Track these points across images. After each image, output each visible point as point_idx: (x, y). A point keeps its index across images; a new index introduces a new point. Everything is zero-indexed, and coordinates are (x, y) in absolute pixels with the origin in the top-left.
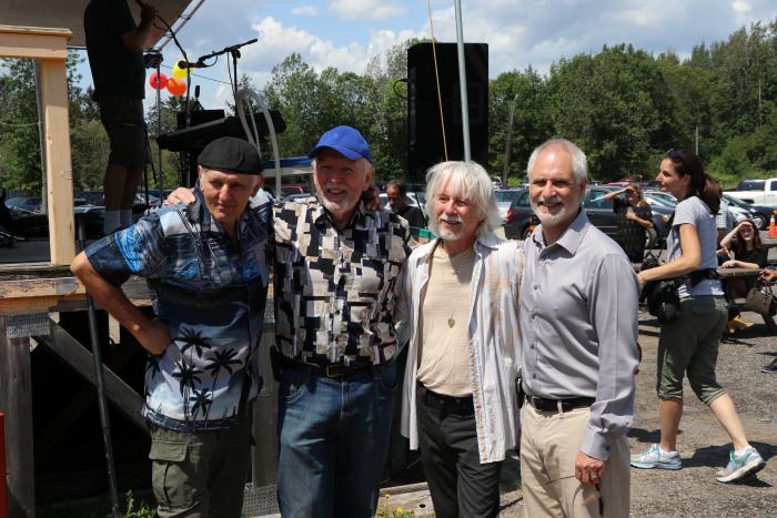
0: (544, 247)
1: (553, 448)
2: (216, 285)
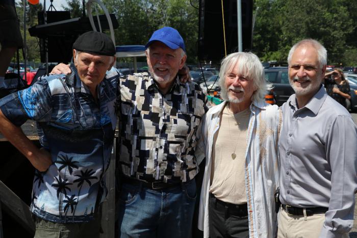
0: (296, 109)
2: (84, 128)
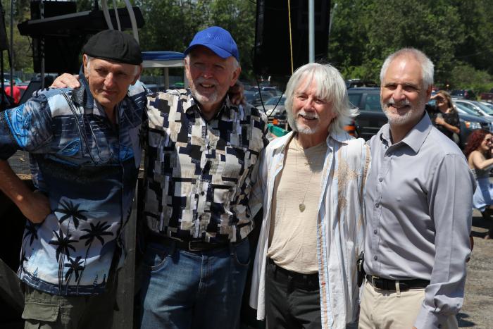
0: (390, 144)
1: (390, 323)
2: (96, 163)
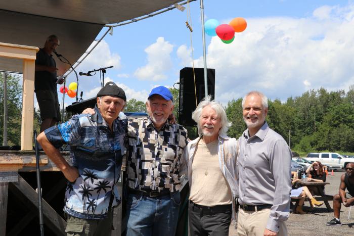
0: (249, 138)
1: (253, 228)
